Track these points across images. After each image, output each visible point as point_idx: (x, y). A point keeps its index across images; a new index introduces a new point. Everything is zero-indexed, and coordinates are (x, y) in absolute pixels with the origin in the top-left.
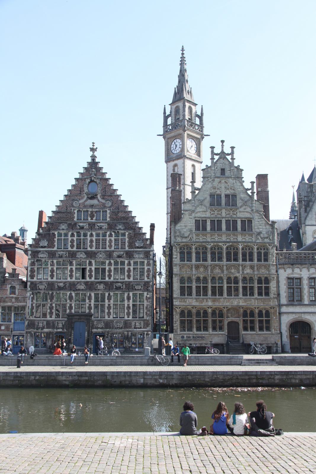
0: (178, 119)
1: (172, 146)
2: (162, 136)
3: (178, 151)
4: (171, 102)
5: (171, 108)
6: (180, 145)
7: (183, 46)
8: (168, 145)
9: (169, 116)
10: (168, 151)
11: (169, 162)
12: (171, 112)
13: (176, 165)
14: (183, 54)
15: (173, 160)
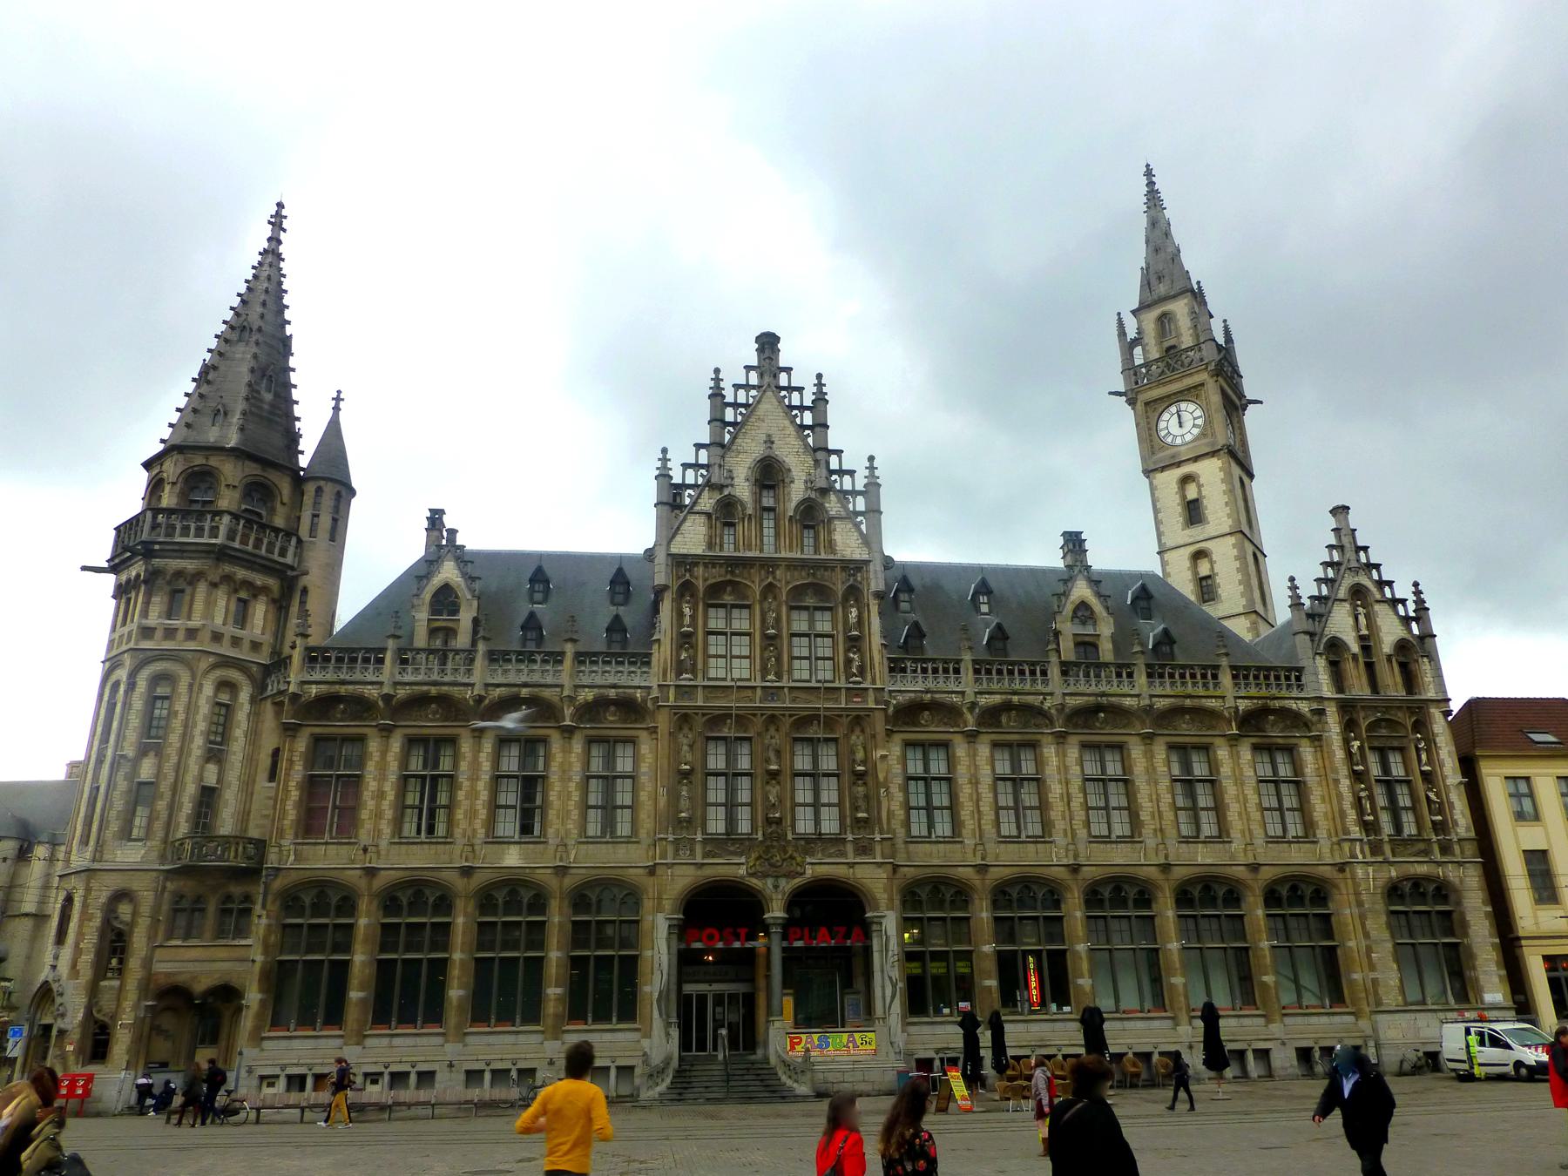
0: (1173, 347)
1: (1162, 425)
2: (1124, 398)
3: (1188, 438)
4: (1136, 305)
5: (1139, 322)
6: (1195, 419)
7: (1148, 166)
8: (1148, 423)
9: (1136, 342)
10: (1151, 441)
11: (1163, 469)
12: (1140, 331)
13: (1186, 480)
14: (1151, 184)
15: (1179, 464)
